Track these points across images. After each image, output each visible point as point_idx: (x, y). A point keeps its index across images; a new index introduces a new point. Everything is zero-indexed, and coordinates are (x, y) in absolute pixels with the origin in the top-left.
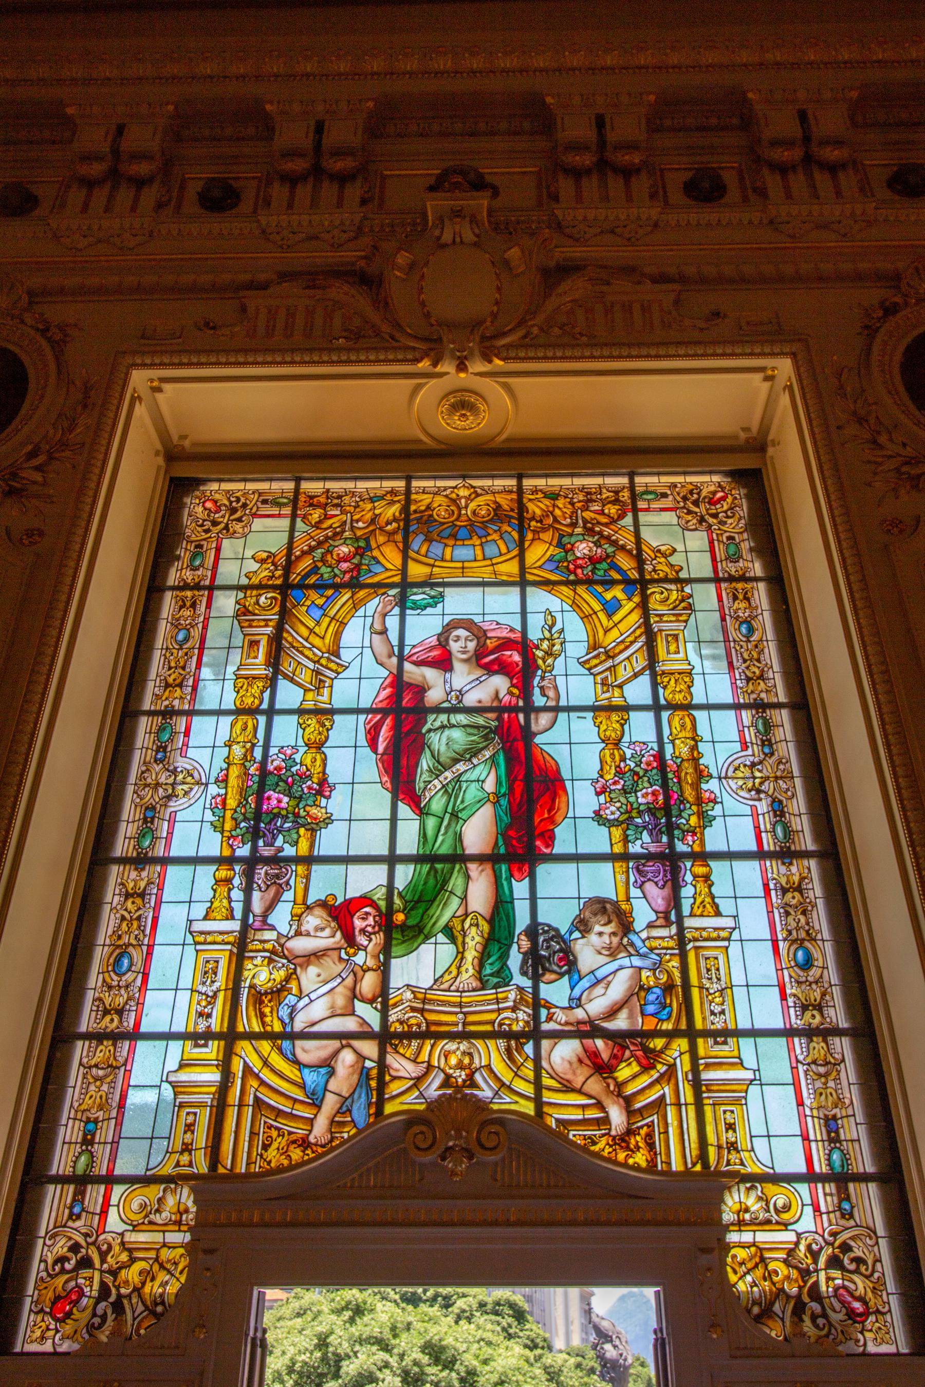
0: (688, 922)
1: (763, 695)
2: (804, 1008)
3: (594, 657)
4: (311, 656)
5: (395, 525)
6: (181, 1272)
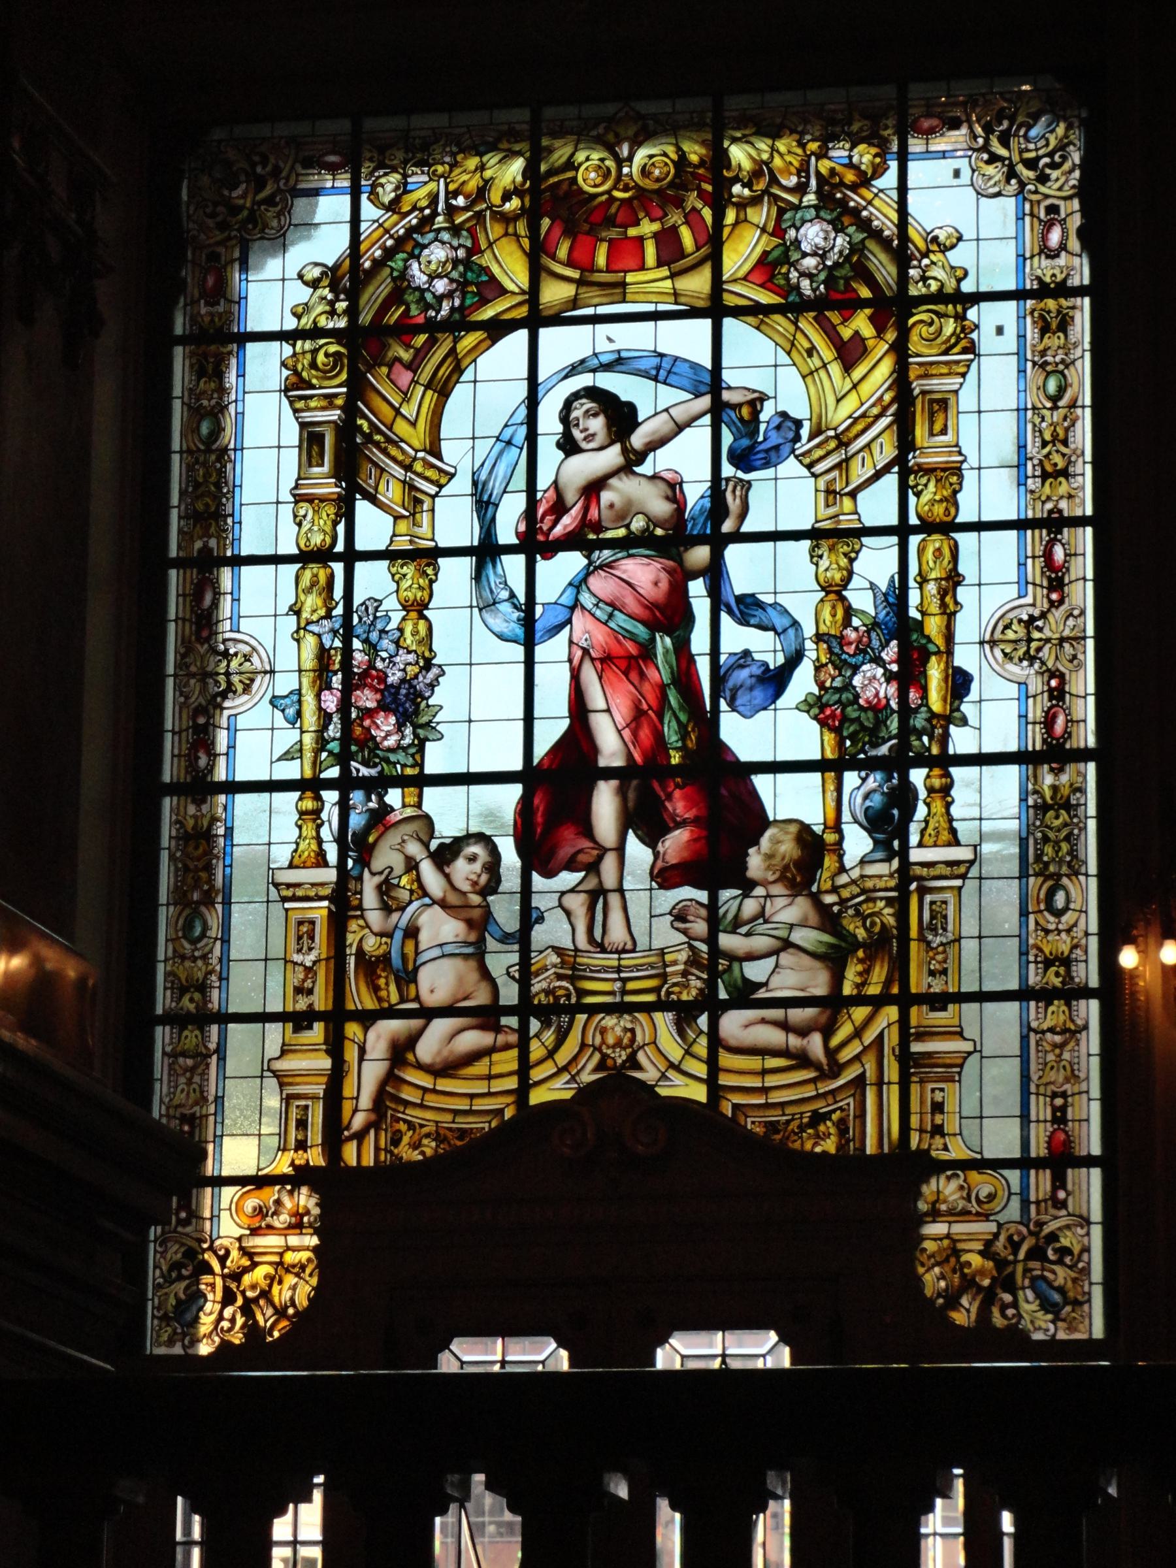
0: (916, 855)
1: (1063, 505)
2: (1048, 963)
3: (818, 446)
4: (401, 458)
5: (514, 204)
6: (311, 1275)
